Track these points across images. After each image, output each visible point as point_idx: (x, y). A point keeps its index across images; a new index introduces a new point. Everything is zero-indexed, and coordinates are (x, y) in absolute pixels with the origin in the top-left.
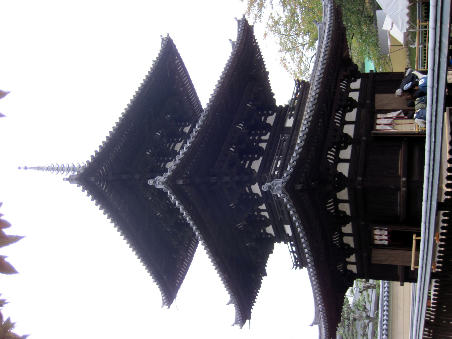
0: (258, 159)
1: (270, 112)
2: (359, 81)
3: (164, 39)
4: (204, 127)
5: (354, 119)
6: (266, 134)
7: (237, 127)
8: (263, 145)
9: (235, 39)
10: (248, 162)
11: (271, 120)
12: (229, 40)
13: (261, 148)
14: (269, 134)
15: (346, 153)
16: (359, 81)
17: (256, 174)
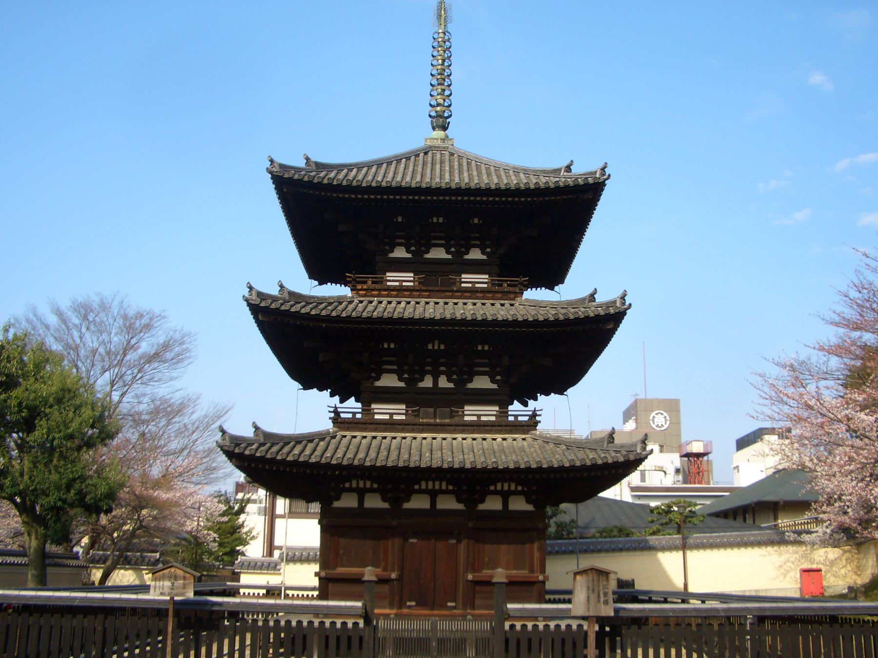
0: (400, 379)
1: (498, 378)
2: (530, 508)
3: (596, 174)
5: (440, 506)
6: (449, 380)
7: (436, 342)
8: (427, 383)
9: (600, 298)
11: (482, 383)
12: (596, 289)
13: (422, 380)
14: (451, 385)
15: (374, 502)
16: (530, 508)
17: (368, 384)
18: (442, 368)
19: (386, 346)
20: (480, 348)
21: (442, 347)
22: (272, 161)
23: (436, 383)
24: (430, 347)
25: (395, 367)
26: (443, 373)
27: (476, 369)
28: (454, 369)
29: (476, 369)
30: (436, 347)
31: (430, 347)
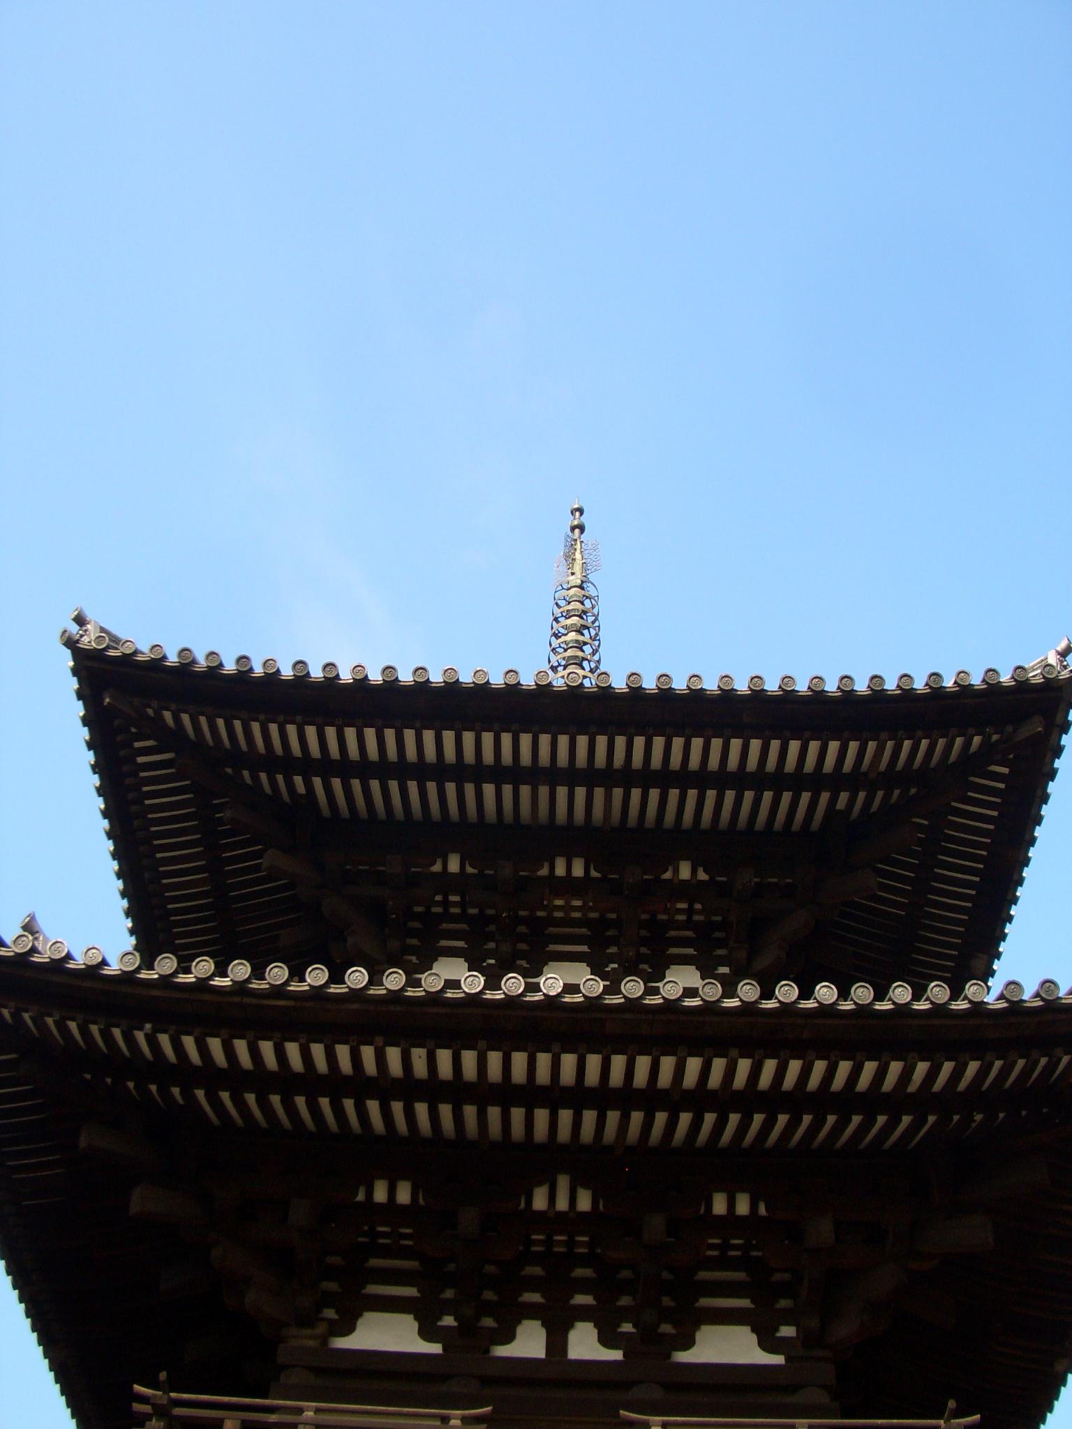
1: (787, 1331)
4: (247, 1000)
6: (606, 1340)
7: (563, 1183)
10: (411, 1292)
13: (509, 1337)
18: (582, 1299)
19: (380, 1195)
20: (719, 1206)
21: (584, 1203)
22: (80, 620)
23: (557, 1343)
24: (540, 1202)
25: (411, 1292)
26: (583, 1314)
27: (705, 1302)
28: (625, 1301)
29: (705, 1302)
30: (562, 1204)
31: (540, 1202)
